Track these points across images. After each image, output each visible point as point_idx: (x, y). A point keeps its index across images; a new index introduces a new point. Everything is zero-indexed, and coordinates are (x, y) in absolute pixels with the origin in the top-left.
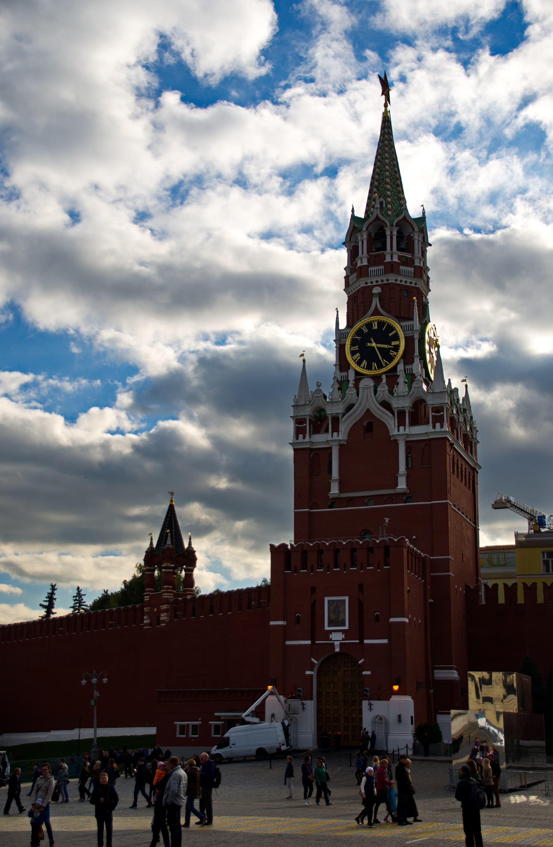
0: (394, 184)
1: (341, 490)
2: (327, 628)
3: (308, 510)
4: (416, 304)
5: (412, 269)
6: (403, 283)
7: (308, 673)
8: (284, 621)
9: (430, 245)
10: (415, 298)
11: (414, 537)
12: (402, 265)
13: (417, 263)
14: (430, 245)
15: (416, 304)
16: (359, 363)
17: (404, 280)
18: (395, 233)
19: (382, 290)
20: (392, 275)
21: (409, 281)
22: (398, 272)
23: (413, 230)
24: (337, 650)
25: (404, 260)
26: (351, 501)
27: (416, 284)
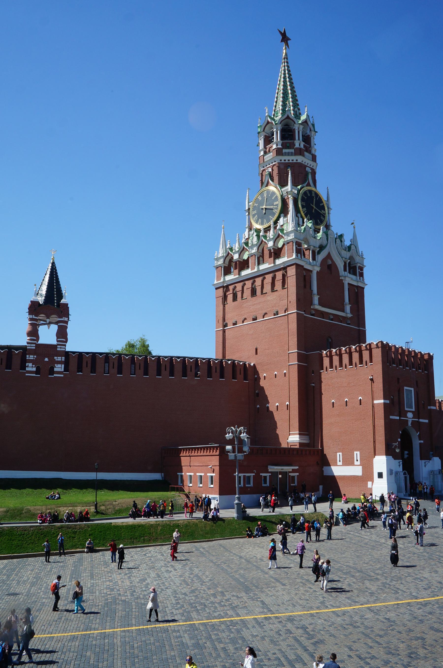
4: (290, 173)
5: (292, 151)
6: (287, 161)
9: (317, 132)
10: (289, 169)
13: (297, 145)
14: (317, 132)
16: (257, 222)
17: (287, 158)
19: (272, 169)
23: (295, 123)
25: (288, 145)
27: (297, 160)
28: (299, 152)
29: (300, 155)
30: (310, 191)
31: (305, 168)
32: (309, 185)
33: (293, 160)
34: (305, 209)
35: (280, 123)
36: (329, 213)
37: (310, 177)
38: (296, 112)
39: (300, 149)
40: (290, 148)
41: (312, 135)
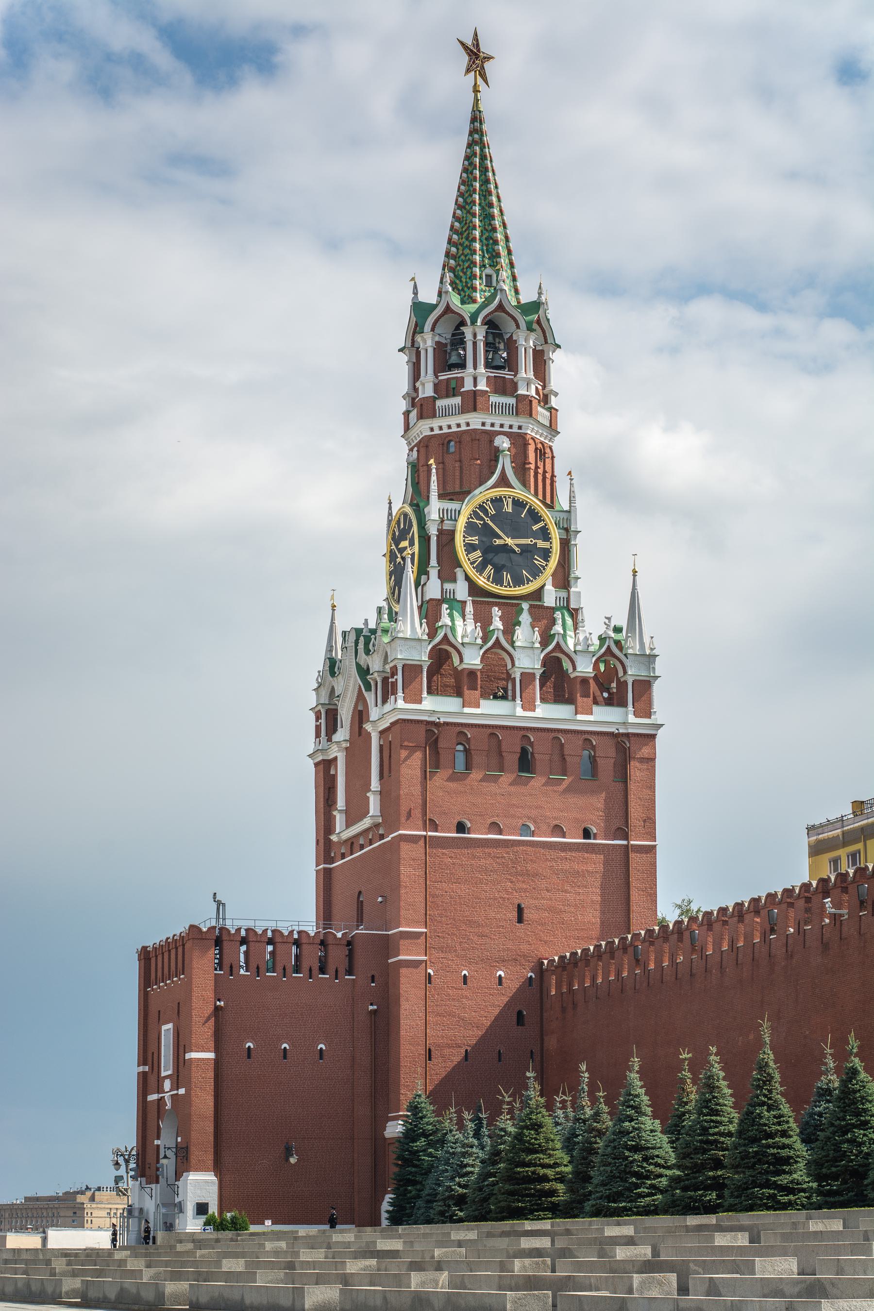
0: (467, 239)
1: (349, 824)
2: (163, 1074)
3: (321, 866)
4: (434, 471)
5: (457, 400)
6: (445, 430)
7: (156, 1142)
8: (145, 1064)
10: (432, 461)
11: (380, 899)
12: (441, 397)
13: (468, 386)
15: (434, 471)
17: (444, 422)
18: (429, 343)
19: (418, 451)
20: (421, 423)
21: (453, 421)
22: (434, 416)
24: (169, 1106)
26: (352, 844)
27: (468, 424)
28: (472, 402)
29: (475, 410)
30: (497, 501)
31: (491, 441)
32: (503, 481)
33: (459, 425)
34: (478, 553)
35: (433, 329)
36: (566, 545)
37: (505, 463)
38: (489, 277)
39: (475, 393)
40: (454, 395)
41: (521, 342)
